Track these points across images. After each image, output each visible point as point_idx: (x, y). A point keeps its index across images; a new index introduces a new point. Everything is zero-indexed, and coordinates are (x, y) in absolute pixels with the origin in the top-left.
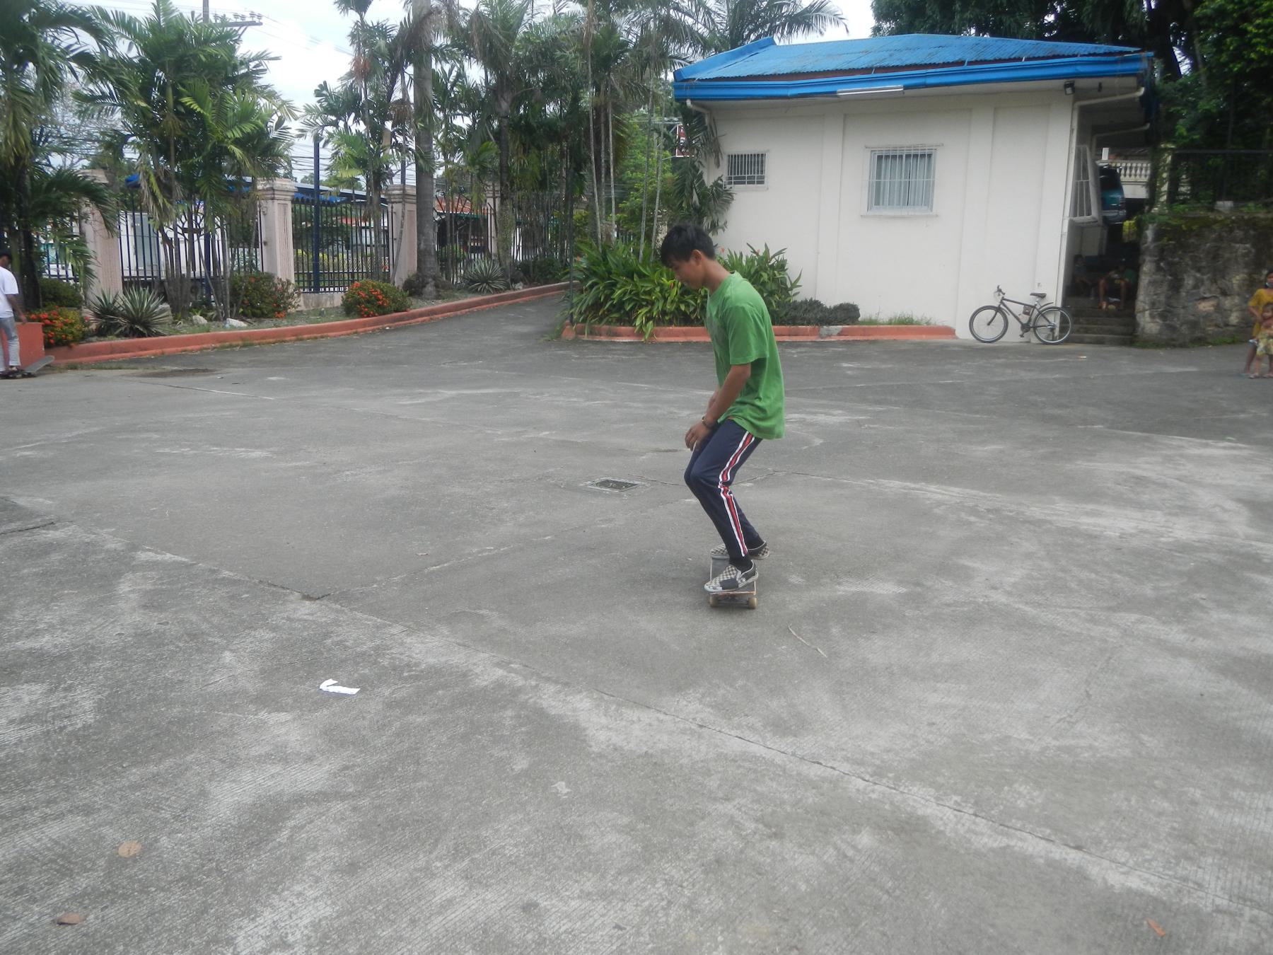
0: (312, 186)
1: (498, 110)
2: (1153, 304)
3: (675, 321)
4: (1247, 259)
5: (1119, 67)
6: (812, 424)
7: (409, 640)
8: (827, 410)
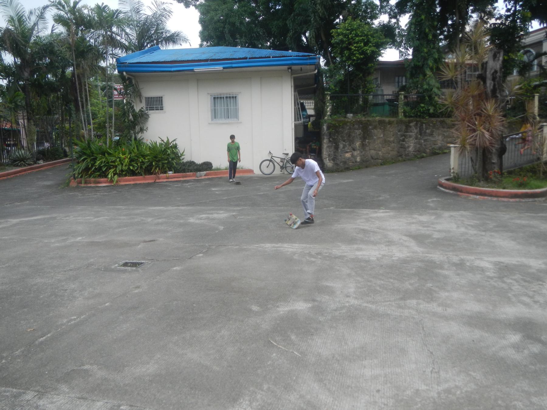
1: (23, 76)
2: (329, 155)
3: (128, 174)
4: (360, 136)
5: (308, 61)
6: (214, 219)
7: (41, 403)
8: (216, 212)
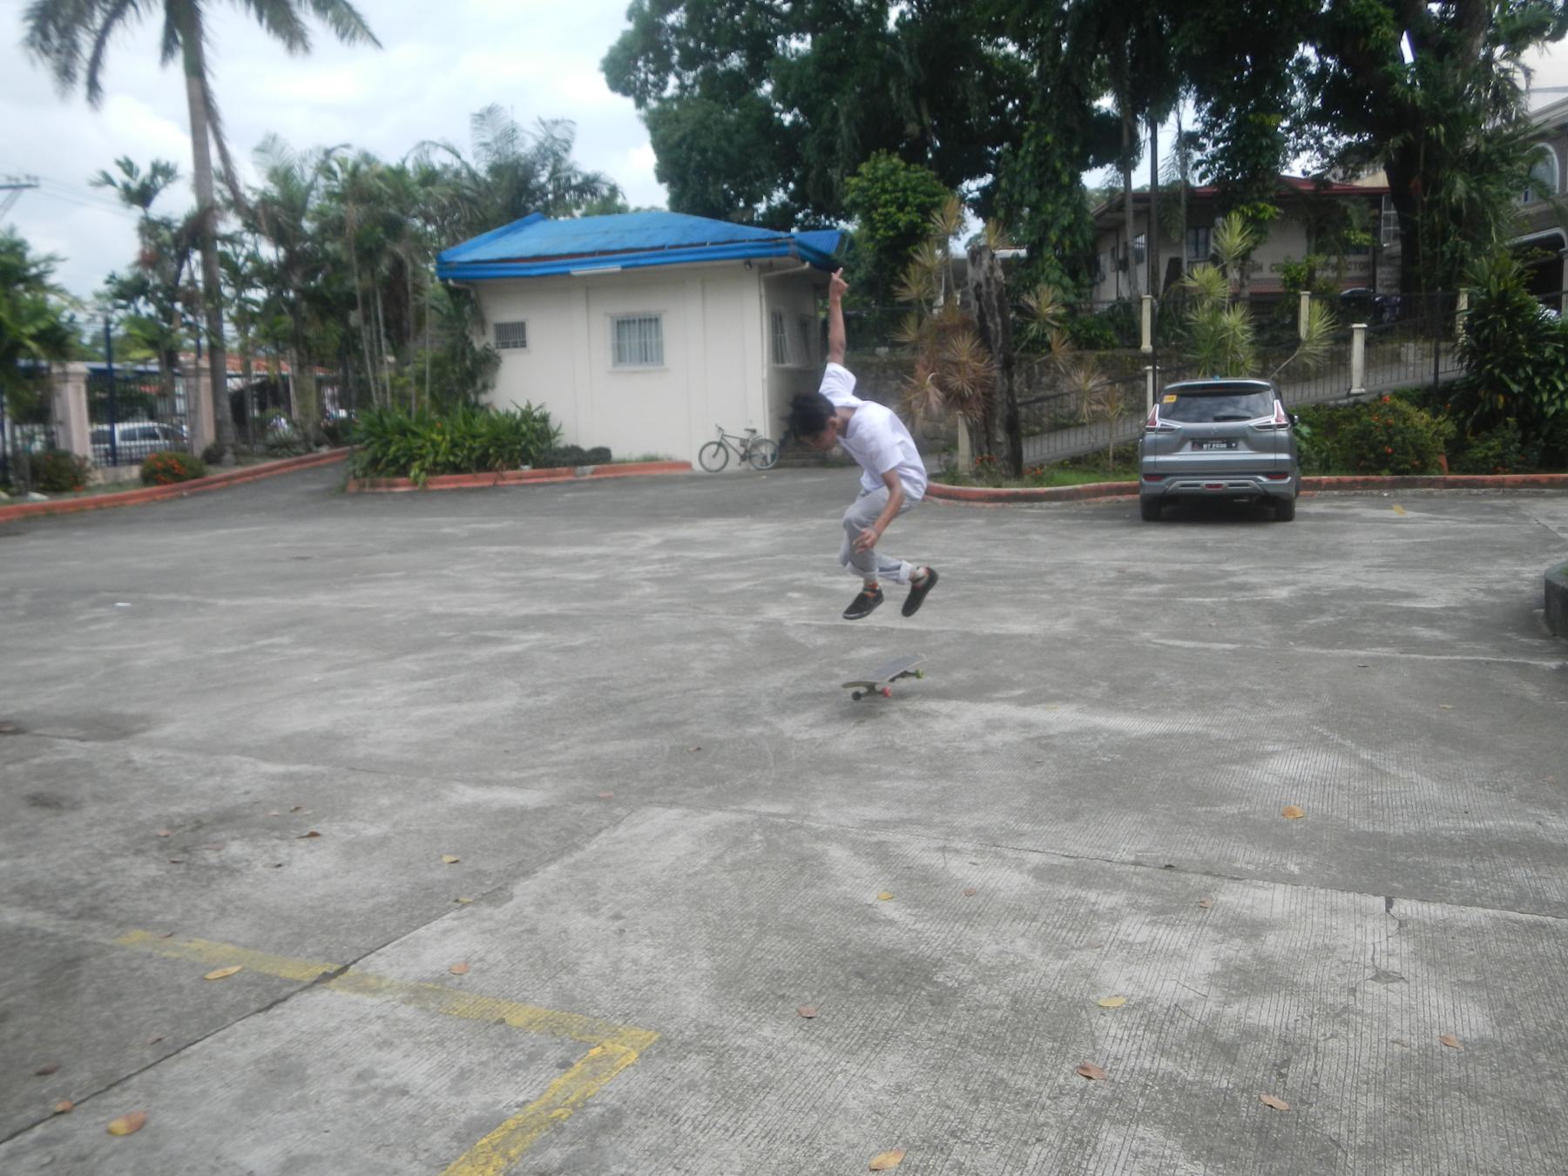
0: (103, 365)
5: (775, 250)
